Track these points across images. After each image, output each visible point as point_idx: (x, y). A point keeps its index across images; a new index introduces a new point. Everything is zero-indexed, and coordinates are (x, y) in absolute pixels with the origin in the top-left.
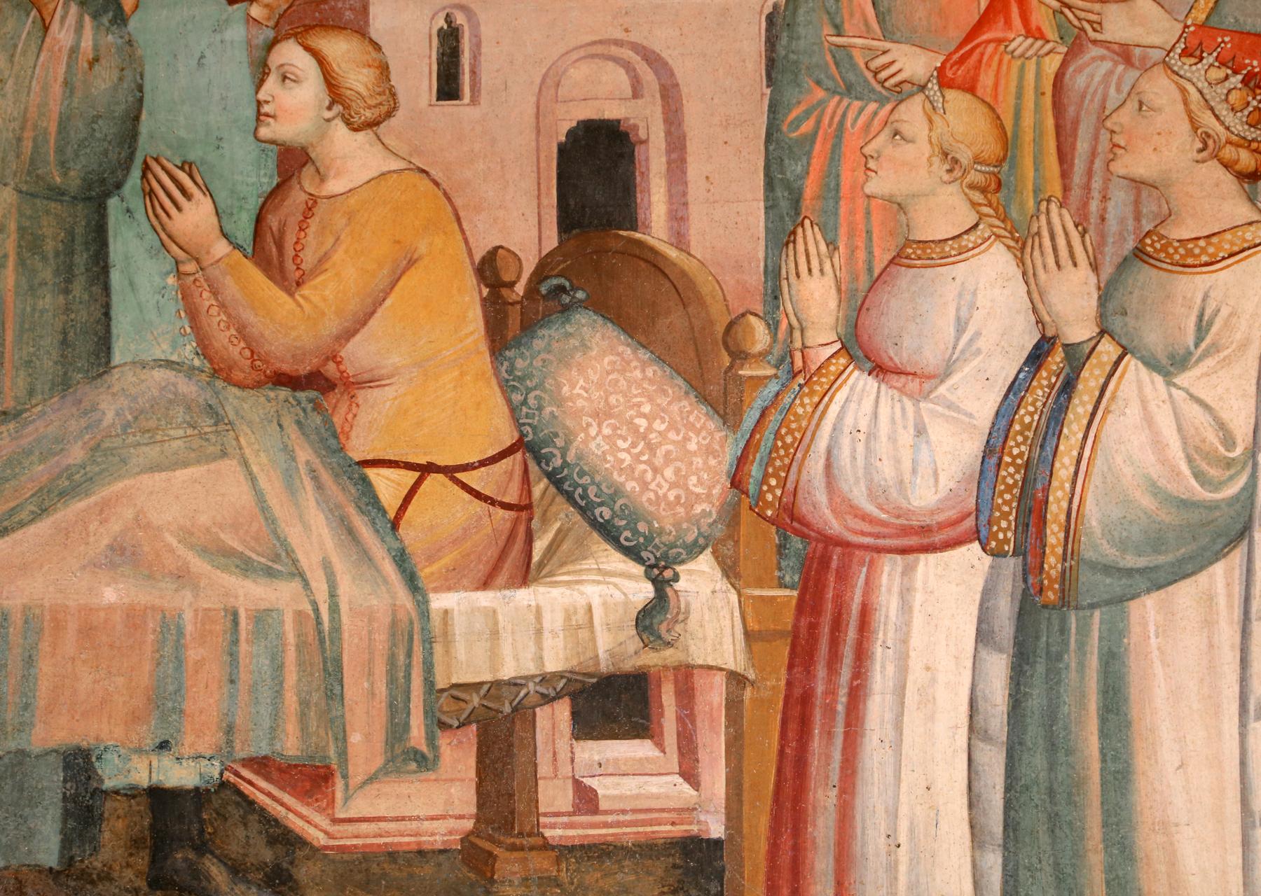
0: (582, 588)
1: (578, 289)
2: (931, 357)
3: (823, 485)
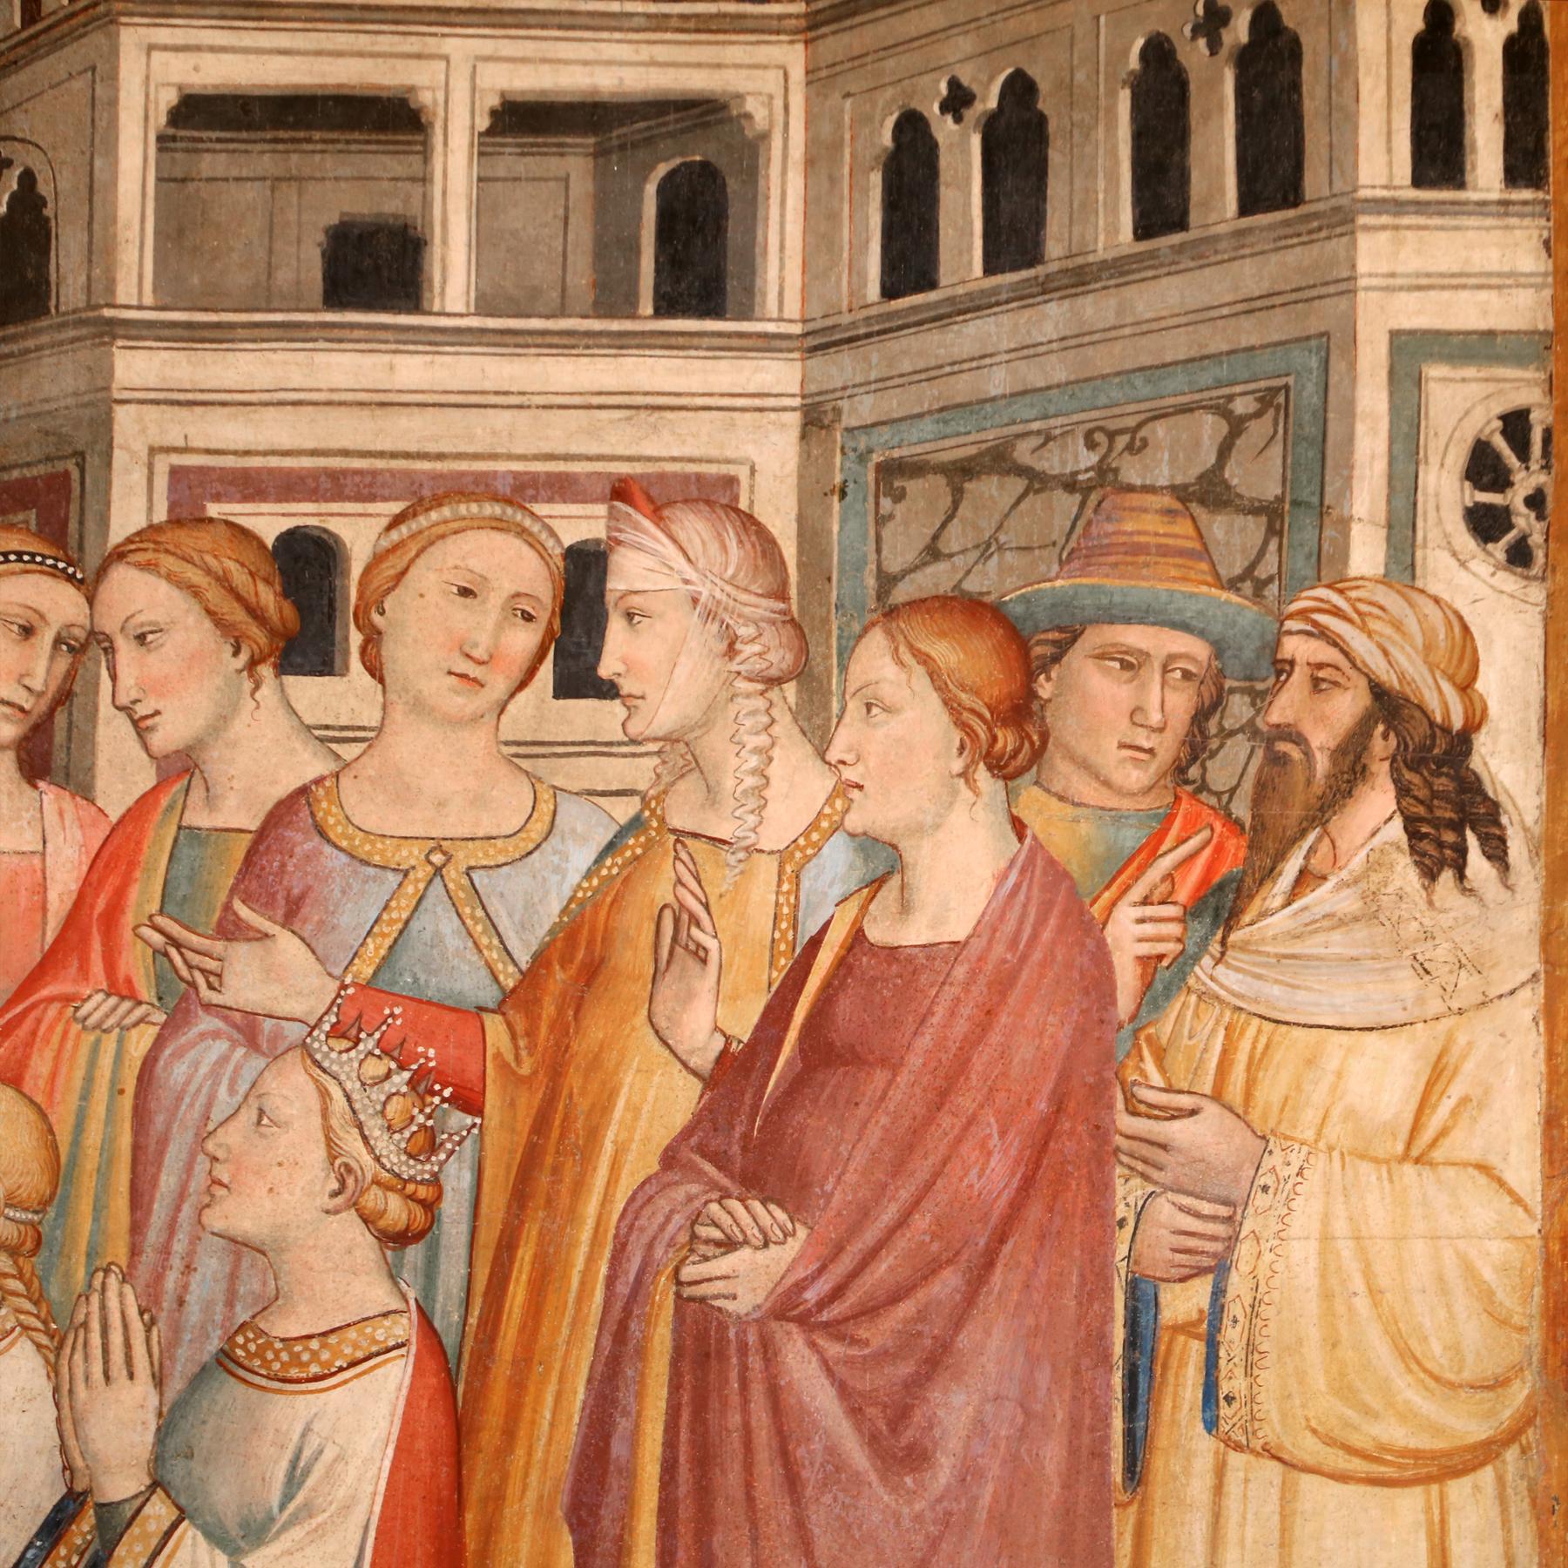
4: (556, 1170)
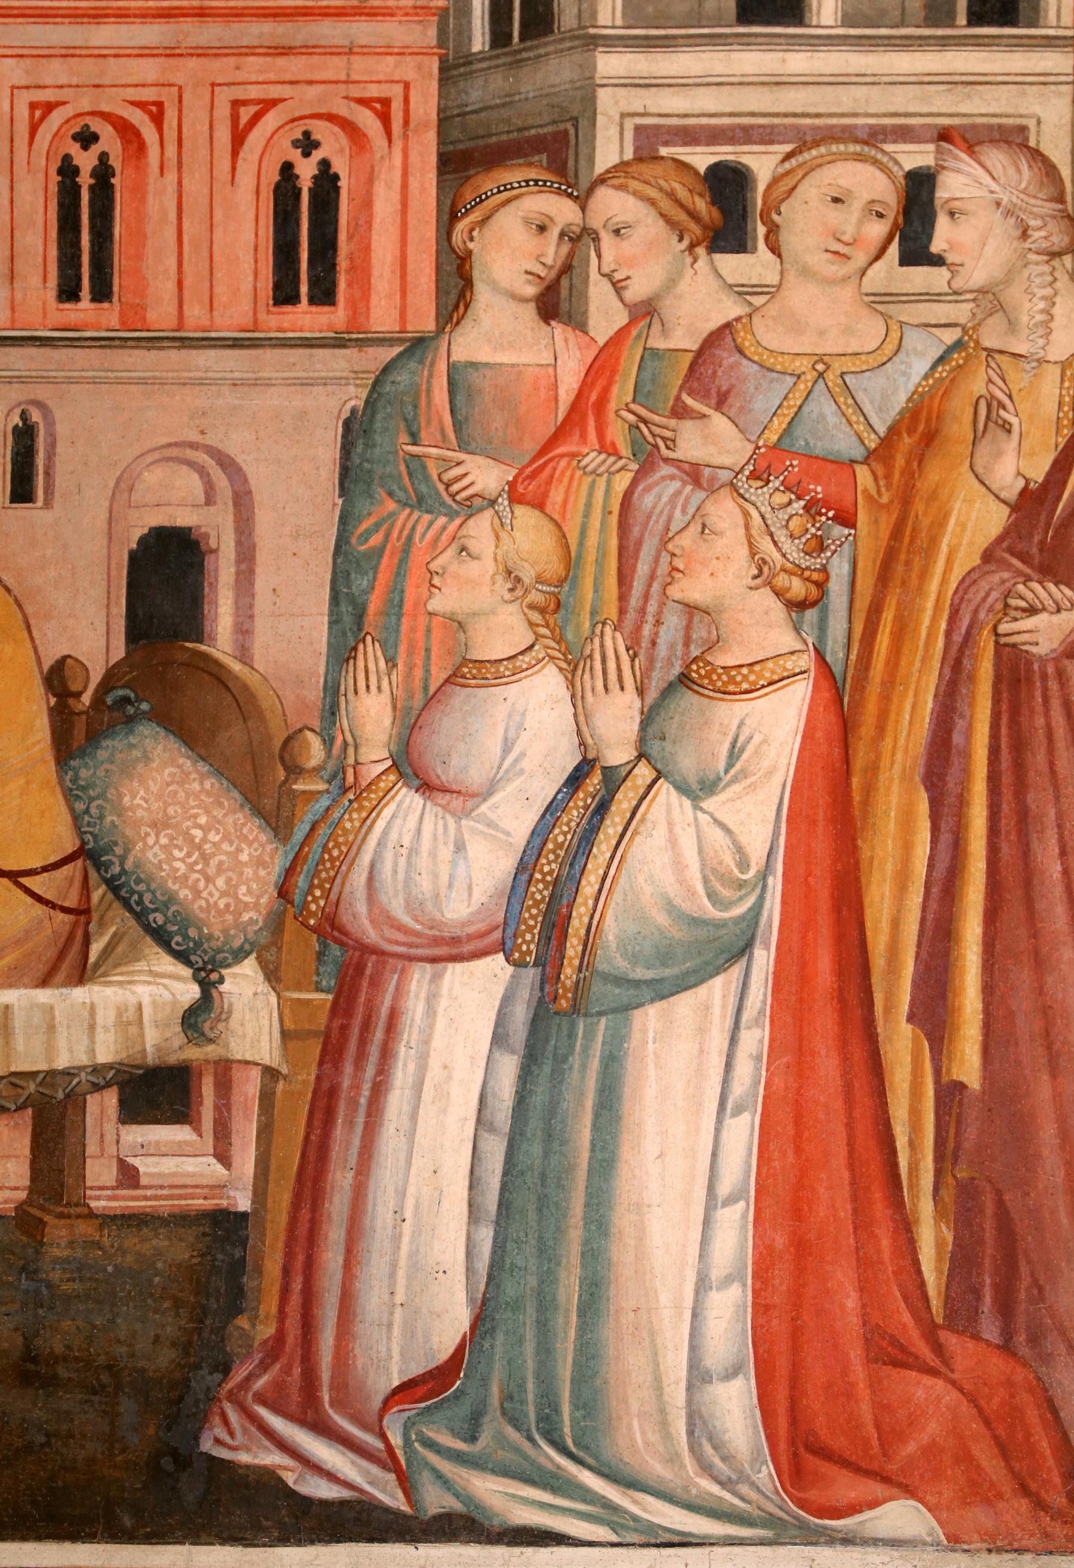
0: (134, 988)
1: (142, 700)
2: (476, 776)
3: (364, 897)
4: (908, 563)
